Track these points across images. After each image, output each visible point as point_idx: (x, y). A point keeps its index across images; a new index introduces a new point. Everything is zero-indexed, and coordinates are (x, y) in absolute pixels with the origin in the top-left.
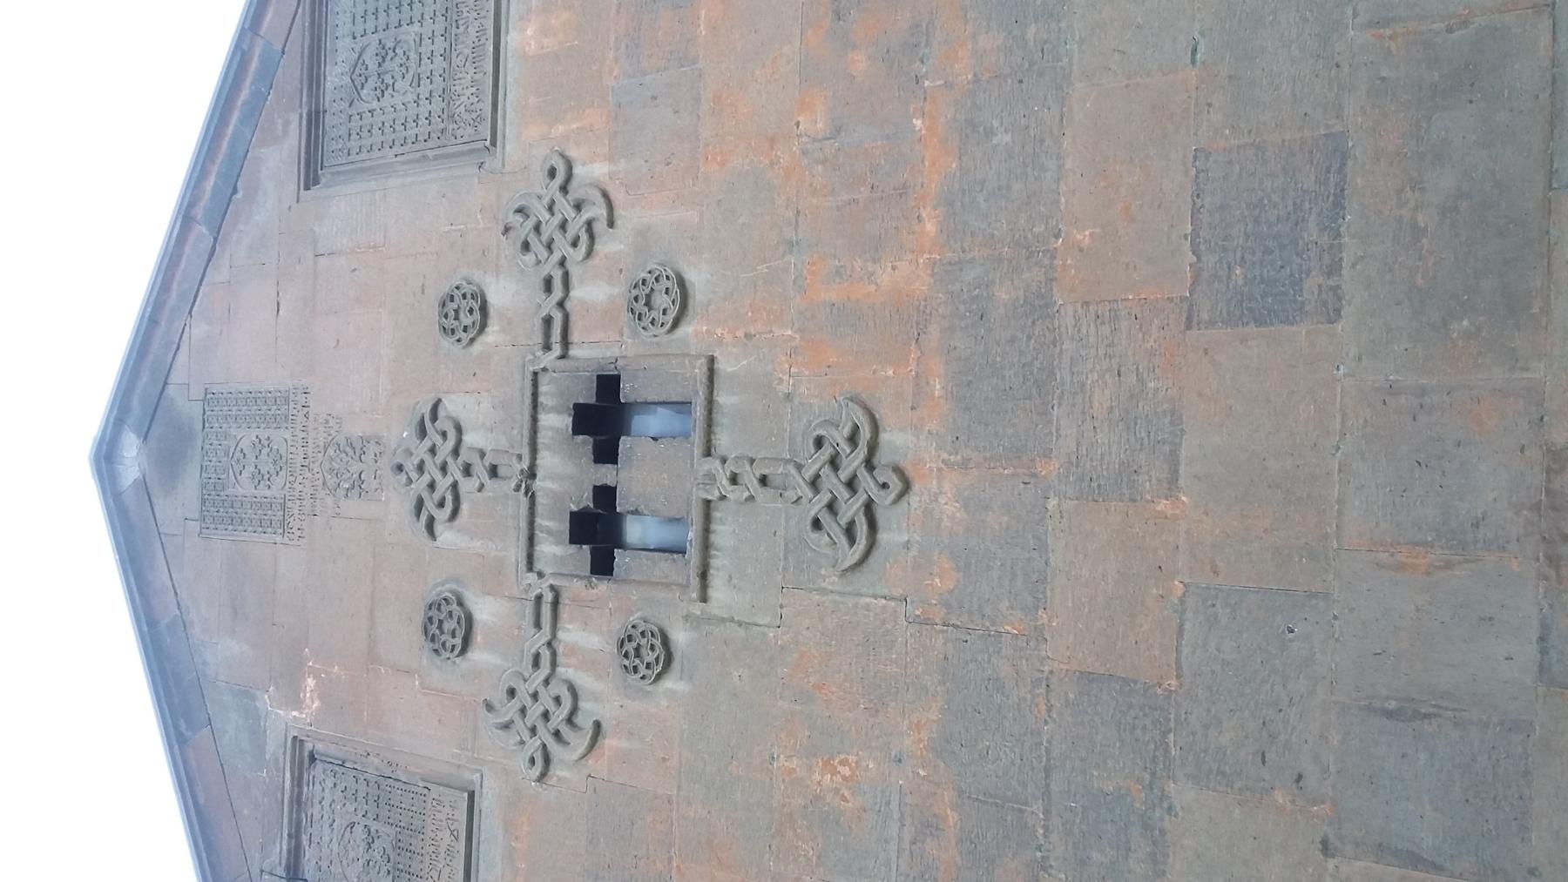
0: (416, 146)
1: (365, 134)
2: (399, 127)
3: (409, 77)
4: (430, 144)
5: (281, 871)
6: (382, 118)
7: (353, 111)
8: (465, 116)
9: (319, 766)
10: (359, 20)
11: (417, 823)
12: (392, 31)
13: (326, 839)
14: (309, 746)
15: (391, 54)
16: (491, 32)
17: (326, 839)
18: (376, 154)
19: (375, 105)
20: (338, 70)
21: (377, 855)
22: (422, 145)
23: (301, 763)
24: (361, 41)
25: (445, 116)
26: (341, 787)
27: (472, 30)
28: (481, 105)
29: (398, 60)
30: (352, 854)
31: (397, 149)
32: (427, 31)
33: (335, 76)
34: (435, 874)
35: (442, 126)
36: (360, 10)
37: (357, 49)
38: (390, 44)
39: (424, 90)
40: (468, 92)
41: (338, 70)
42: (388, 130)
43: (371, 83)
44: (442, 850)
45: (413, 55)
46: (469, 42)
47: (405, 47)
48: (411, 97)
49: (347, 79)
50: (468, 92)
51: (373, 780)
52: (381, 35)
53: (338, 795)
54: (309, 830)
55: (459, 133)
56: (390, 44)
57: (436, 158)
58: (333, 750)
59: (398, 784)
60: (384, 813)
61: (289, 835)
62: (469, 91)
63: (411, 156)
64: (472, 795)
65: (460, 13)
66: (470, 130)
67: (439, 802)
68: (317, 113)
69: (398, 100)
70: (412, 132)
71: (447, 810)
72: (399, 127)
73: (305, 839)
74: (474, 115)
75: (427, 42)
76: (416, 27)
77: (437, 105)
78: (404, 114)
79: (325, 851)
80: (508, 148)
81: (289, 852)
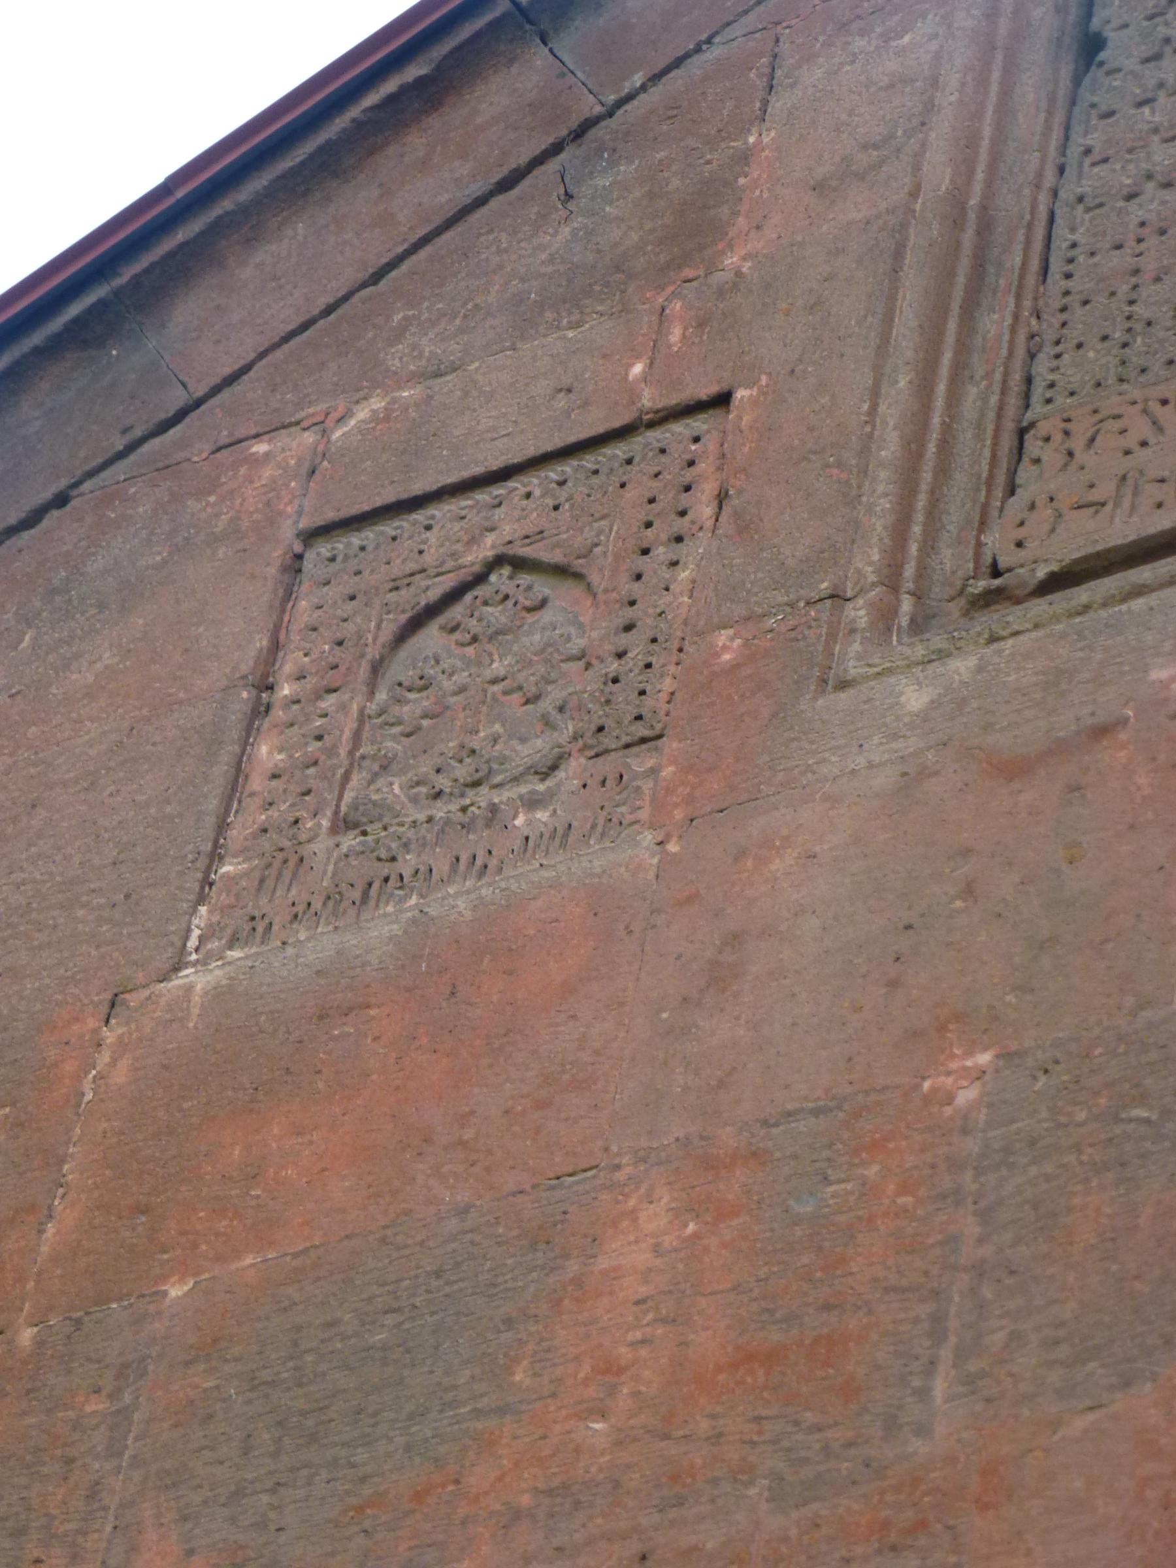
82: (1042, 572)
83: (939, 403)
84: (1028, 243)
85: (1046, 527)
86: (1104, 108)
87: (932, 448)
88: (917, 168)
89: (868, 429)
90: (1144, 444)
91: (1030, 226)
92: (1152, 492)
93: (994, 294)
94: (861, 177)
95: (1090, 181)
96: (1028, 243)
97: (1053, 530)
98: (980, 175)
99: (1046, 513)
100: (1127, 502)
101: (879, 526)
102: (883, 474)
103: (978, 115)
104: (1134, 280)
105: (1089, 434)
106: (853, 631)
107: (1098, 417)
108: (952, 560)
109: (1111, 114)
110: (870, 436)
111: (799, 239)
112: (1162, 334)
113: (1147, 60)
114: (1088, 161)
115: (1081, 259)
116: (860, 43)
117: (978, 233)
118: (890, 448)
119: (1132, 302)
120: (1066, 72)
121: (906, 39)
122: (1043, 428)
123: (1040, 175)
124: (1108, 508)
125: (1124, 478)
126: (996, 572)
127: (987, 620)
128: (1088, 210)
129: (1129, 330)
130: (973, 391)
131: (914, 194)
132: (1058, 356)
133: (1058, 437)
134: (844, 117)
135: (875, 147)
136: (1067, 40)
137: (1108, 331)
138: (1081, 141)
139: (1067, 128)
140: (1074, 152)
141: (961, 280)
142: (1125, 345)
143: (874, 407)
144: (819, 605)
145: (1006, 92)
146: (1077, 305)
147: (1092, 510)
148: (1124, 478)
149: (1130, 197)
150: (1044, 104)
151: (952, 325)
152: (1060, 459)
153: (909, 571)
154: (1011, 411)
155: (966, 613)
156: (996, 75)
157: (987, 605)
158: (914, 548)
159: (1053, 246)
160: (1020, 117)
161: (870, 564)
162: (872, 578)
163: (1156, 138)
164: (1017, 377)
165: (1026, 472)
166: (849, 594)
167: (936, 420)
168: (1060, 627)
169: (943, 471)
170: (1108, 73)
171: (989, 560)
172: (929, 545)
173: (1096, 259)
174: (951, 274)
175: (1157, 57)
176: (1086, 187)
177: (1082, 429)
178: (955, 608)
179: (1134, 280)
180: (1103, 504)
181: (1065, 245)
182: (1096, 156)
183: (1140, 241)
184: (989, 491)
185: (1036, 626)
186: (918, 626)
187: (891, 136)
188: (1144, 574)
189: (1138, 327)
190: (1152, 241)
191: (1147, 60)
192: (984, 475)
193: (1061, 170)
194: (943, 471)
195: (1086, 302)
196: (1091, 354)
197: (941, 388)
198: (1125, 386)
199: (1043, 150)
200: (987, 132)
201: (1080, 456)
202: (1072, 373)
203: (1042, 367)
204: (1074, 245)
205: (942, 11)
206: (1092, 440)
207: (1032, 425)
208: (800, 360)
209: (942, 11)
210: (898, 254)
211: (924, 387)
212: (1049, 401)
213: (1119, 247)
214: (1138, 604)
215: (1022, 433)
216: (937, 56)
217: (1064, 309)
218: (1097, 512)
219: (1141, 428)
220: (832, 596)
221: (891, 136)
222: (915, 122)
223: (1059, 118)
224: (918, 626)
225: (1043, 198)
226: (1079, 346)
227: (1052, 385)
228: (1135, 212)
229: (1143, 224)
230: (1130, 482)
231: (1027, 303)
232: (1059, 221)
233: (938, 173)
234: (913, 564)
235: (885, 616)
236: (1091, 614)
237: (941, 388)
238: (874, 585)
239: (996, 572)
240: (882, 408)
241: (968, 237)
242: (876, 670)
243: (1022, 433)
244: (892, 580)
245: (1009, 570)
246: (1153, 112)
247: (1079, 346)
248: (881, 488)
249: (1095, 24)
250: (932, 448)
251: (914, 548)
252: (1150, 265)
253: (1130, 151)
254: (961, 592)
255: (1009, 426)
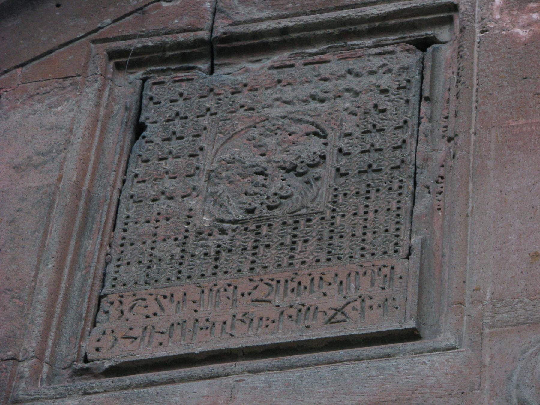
5: (222, 27)
9: (410, 59)
11: (346, 245)
13: (289, 93)
14: (443, 34)
17: (289, 93)
21: (276, 185)
23: (413, 27)
26: (383, 101)
30: (271, 142)
34: (262, 292)
44: (309, 299)
51: (408, 153)
53: (368, 100)
54: (299, 62)
58: (445, 76)
59: (406, 200)
60: (352, 184)
61: (285, 30)
64: (412, 335)
67: (389, 278)
71: (378, 296)
73: (284, 56)
79: (269, 96)
81: (257, 35)
82: (107, 365)
83: (65, 278)
84: (108, 212)
85: (110, 344)
86: (144, 157)
87: (61, 297)
88: (61, 169)
89: (33, 284)
90: (155, 314)
91: (109, 205)
92: (158, 337)
93: (91, 230)
94: (36, 167)
95: (136, 189)
96: (108, 212)
97: (113, 346)
98: (88, 177)
99: (109, 338)
100: (147, 339)
101: (36, 331)
102: (39, 307)
103: (89, 149)
104: (154, 239)
105: (131, 305)
106: (22, 377)
107: (135, 298)
108: (67, 352)
109: (147, 161)
110: (34, 287)
111: (6, 189)
112: (165, 266)
113: (164, 140)
114: (136, 180)
115: (131, 224)
116: (38, 106)
117: (86, 203)
118: (43, 295)
119: (152, 248)
120: (129, 137)
121: (59, 109)
122: (111, 298)
123: (115, 182)
124: (138, 340)
125: (145, 328)
126: (86, 361)
127: (81, 383)
128: (135, 202)
129: (151, 261)
130: (79, 274)
131: (60, 180)
132: (118, 266)
133: (117, 303)
134: (29, 138)
135: (43, 155)
136: (130, 124)
137: (141, 260)
138: (133, 170)
139: (128, 163)
140: (130, 176)
141: (78, 223)
142: (149, 267)
143: (37, 274)
144: (7, 362)
145: (101, 141)
146: (128, 245)
147: (131, 340)
148: (145, 328)
149: (154, 200)
150: (118, 151)
151: (72, 243)
152: (118, 314)
153: (48, 353)
154: (97, 288)
155: (71, 377)
156: (98, 133)
157: (81, 375)
158: (50, 343)
159: (119, 216)
160: (106, 153)
161: (32, 347)
162: (32, 354)
163: (167, 176)
164: (100, 272)
165: (101, 316)
166: (21, 359)
167: (63, 285)
168: (116, 394)
169: (65, 309)
170: (147, 142)
171: (84, 355)
172: (56, 343)
173: (138, 225)
174: (74, 220)
175: (169, 139)
176: (135, 191)
177: (128, 302)
178: (66, 373)
179: (154, 239)
180: (136, 339)
181: (124, 216)
182: (140, 178)
183: (157, 221)
184: (85, 323)
185: (105, 391)
186: (50, 379)
187: (50, 151)
188: (154, 376)
189: (155, 260)
190: (163, 222)
191: (164, 140)
192: (84, 315)
193: (124, 181)
194: (65, 309)
195: (132, 244)
196: (133, 269)
197: (66, 271)
198: (148, 286)
199: (116, 171)
200: (92, 158)
201: (127, 314)
202: (124, 275)
203: (111, 269)
204: (128, 217)
205: (76, 99)
206: (132, 308)
207: (106, 295)
208: (4, 246)
209: (76, 99)
210: (51, 206)
211: (59, 270)
212: (114, 286)
213: (148, 222)
214: (152, 389)
215: (100, 298)
216: (73, 119)
217: (122, 245)
218: (133, 342)
219: (154, 307)
220: (13, 359)
221: (50, 151)
222: (62, 147)
223: (125, 158)
224: (50, 379)
225: (116, 193)
226: (128, 264)
227: (115, 279)
228: (157, 207)
229: (159, 214)
230: (148, 331)
231: (106, 239)
232: (122, 205)
233: (71, 173)
234: (50, 350)
235: (36, 372)
236: (130, 391)
237: (66, 271)
238: (33, 357)
239: (86, 361)
240: (40, 275)
241: (82, 203)
242: (32, 397)
243: (100, 298)
244: (40, 357)
245: (93, 361)
246: (166, 164)
247: (128, 264)
248: (38, 313)
249: (142, 118)
250: (61, 297)
251: (50, 343)
252: (162, 234)
253: (155, 179)
254: (70, 367)
255: (96, 294)
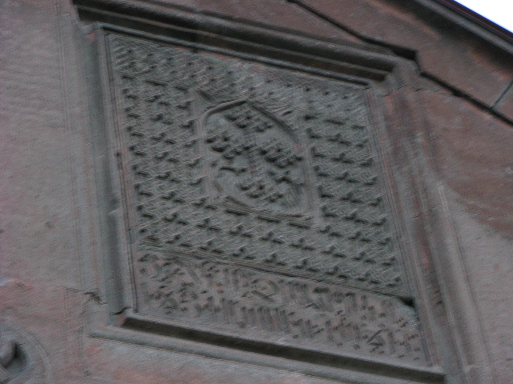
0: (131, 191)
1: (156, 110)
2: (164, 167)
3: (242, 197)
4: (134, 214)
6: (180, 143)
7: (193, 97)
8: (176, 283)
10: (334, 131)
12: (315, 182)
15: (280, 173)
16: (307, 345)
18: (124, 122)
19: (202, 134)
20: (259, 84)
22: (134, 201)
24: (301, 127)
25: (176, 247)
27: (310, 314)
28: (192, 311)
29: (269, 183)
31: (128, 158)
32: (313, 239)
33: (249, 76)
35: (163, 239)
36: (349, 134)
37: (290, 120)
38: (295, 174)
39: (221, 219)
40: (213, 292)
41: (259, 84)
42: (161, 148)
43: (236, 134)
45: (276, 209)
46: (292, 306)
47: (289, 199)
48: (211, 195)
49: (242, 95)
50: (213, 292)
52: (309, 163)
55: (149, 266)
56: (295, 174)
57: (112, 222)
62: (214, 295)
63: (116, 181)
65: (339, 297)
66: (153, 286)
68: (193, 38)
69: (206, 173)
70: (154, 187)
72: (164, 167)
74: (176, 297)
75: (296, 236)
76: (319, 223)
77: (198, 238)
78: (184, 178)
80: (122, 349)
